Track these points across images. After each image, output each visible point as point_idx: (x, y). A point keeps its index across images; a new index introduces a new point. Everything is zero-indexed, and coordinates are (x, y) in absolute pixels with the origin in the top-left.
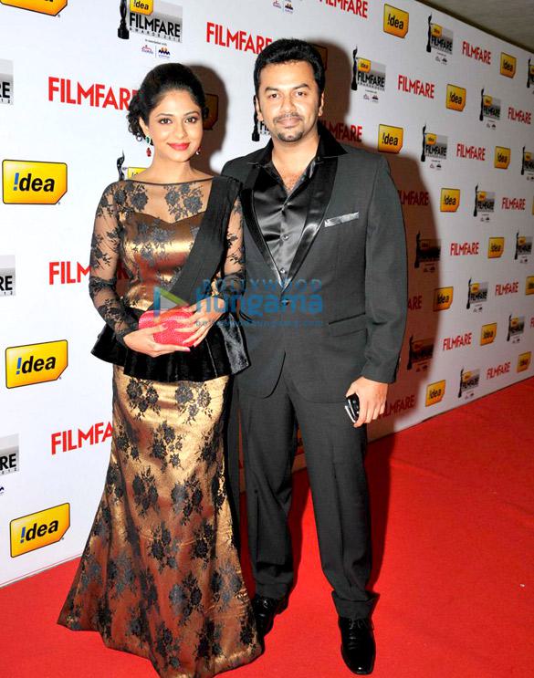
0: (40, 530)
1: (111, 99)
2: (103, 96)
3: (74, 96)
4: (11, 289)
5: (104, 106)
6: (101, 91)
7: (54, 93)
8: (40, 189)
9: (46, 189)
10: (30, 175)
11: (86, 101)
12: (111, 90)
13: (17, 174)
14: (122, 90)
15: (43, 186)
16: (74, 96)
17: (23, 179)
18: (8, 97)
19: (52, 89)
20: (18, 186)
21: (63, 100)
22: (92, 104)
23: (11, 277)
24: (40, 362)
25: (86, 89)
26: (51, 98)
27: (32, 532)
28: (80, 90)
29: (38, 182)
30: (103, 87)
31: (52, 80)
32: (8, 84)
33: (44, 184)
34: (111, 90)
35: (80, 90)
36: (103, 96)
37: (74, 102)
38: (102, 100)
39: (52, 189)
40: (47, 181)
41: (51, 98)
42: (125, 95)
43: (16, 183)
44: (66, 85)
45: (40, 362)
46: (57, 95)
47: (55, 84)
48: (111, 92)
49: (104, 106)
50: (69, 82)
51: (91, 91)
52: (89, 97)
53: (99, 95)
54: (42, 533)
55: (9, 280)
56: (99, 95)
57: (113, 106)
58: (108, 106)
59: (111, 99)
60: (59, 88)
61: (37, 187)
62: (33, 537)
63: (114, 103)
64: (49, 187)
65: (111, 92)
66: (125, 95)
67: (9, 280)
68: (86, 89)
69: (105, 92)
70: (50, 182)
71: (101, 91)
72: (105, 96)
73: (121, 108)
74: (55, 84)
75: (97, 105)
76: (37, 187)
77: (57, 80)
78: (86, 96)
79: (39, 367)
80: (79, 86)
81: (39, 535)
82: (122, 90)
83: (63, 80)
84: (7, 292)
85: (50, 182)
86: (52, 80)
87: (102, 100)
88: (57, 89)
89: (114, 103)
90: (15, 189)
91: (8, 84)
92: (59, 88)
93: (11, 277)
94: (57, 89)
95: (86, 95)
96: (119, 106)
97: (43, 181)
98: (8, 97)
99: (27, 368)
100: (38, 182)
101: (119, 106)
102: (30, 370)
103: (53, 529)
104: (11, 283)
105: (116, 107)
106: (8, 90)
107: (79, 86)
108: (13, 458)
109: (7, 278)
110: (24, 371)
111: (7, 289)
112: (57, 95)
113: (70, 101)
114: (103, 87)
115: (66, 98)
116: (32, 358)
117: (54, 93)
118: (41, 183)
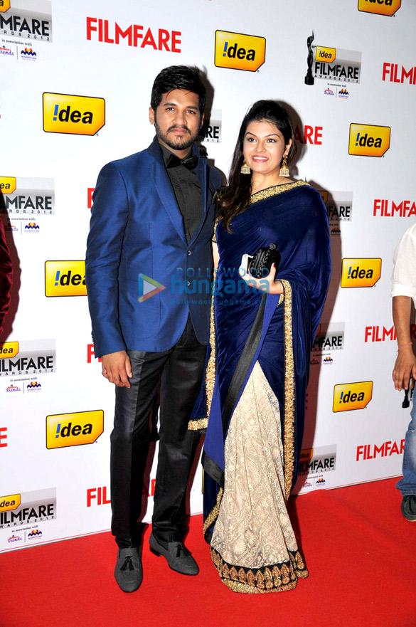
0: (74, 430)
1: (149, 40)
2: (141, 36)
3: (112, 35)
4: (50, 208)
5: (143, 46)
6: (139, 32)
7: (92, 32)
8: (79, 120)
9: (84, 121)
10: (69, 108)
11: (124, 41)
12: (149, 30)
13: (57, 107)
14: (161, 31)
15: (81, 118)
16: (112, 35)
17: (63, 111)
18: (47, 35)
19: (90, 29)
20: (57, 117)
21: (100, 40)
22: (130, 44)
23: (50, 198)
24: (77, 277)
25: (124, 30)
26: (89, 37)
27: (66, 430)
28: (118, 30)
29: (76, 114)
30: (141, 28)
31: (89, 20)
32: (47, 23)
33: (83, 116)
34: (149, 30)
35: (118, 30)
37: (111, 41)
38: (140, 41)
39: (90, 122)
40: (85, 114)
41: (89, 37)
42: (164, 36)
43: (56, 114)
44: (104, 25)
45: (77, 277)
46: (95, 34)
47: (93, 24)
48: (149, 33)
49: (143, 46)
50: (106, 22)
51: (129, 31)
52: (127, 37)
53: (137, 36)
54: (76, 432)
55: (49, 200)
56: (137, 36)
57: (151, 47)
58: (147, 46)
59: (149, 40)
60: (97, 28)
61: (75, 119)
62: (68, 435)
63: (152, 43)
64: (87, 120)
65: (149, 33)
66: (164, 36)
67: (49, 200)
68: (124, 30)
69: (143, 32)
70: (88, 115)
71: (139, 32)
72: (144, 36)
73: (160, 48)
74: (93, 24)
75: (136, 45)
76: (75, 119)
77: (95, 20)
78: (124, 37)
79: (76, 282)
81: (74, 434)
82: (161, 31)
83: (100, 21)
84: (46, 210)
85: (88, 115)
86: (89, 20)
87: (140, 41)
88: (94, 29)
89: (152, 43)
90: (55, 119)
91: (47, 23)
92: (97, 28)
93: (50, 198)
94: (94, 29)
95: (124, 37)
96: (157, 46)
97: (82, 114)
98: (47, 35)
99: (65, 280)
100: (76, 114)
101: (157, 46)
102: (68, 284)
103: (87, 431)
104: (50, 203)
105: (155, 48)
106: (47, 29)
108: (50, 360)
109: (47, 198)
110: (62, 284)
111: (47, 208)
112: (95, 34)
113: (108, 40)
114: (141, 28)
115: (104, 37)
116: (70, 272)
117: (93, 33)
118: (80, 115)
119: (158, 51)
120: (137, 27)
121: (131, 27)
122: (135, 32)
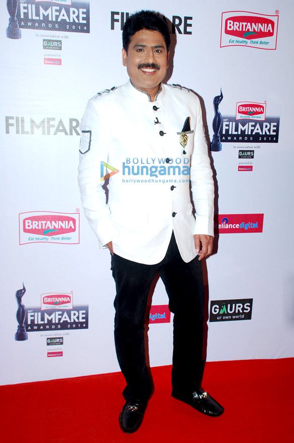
2: (53, 126)
5: (55, 134)
6: (52, 123)
14: (71, 120)
22: (44, 134)
25: (38, 122)
30: (54, 119)
36: (53, 126)
38: (53, 130)
48: (61, 122)
49: (55, 134)
57: (63, 133)
59: (61, 128)
63: (64, 131)
65: (61, 122)
66: (74, 124)
68: (38, 122)
69: (56, 123)
71: (52, 123)
72: (56, 126)
73: (71, 134)
80: (32, 122)
82: (71, 120)
89: (64, 131)
95: (38, 127)
96: (69, 133)
101: (69, 133)
105: (66, 134)
107: (32, 122)
114: (54, 119)
119: (69, 136)
120: (49, 120)
121: (45, 119)
122: (48, 122)
